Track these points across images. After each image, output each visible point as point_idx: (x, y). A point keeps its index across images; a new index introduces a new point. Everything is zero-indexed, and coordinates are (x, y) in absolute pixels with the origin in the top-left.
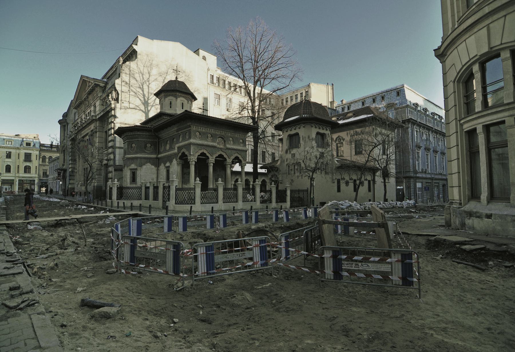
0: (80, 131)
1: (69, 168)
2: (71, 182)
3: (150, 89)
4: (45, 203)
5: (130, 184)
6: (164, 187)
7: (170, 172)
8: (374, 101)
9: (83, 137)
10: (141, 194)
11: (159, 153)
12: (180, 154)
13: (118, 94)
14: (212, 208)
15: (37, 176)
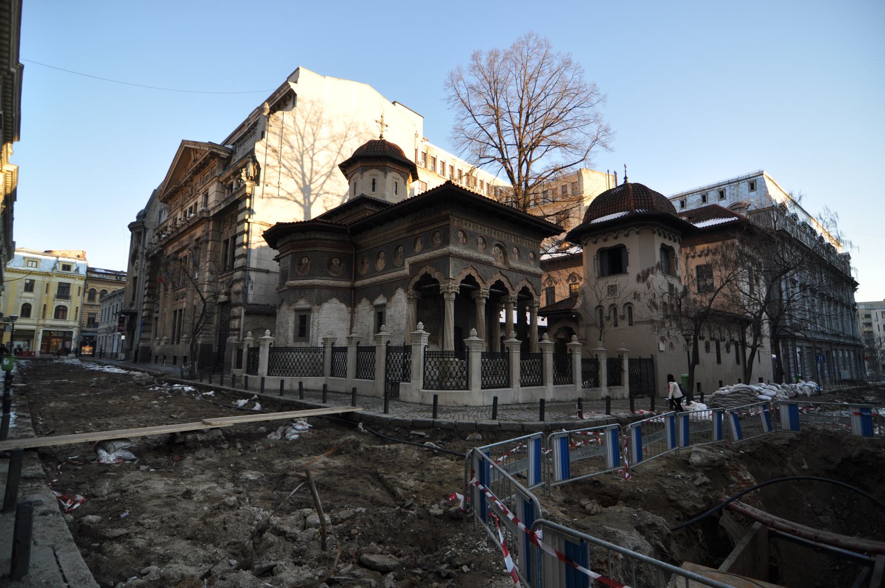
0: (170, 241)
1: (142, 309)
2: (144, 335)
3: (315, 163)
4: (103, 378)
5: (295, 340)
6: (389, 349)
7: (387, 317)
8: (704, 199)
9: (177, 252)
10: (322, 364)
11: (358, 277)
12: (417, 279)
13: (259, 168)
14: (495, 399)
15: (77, 324)
